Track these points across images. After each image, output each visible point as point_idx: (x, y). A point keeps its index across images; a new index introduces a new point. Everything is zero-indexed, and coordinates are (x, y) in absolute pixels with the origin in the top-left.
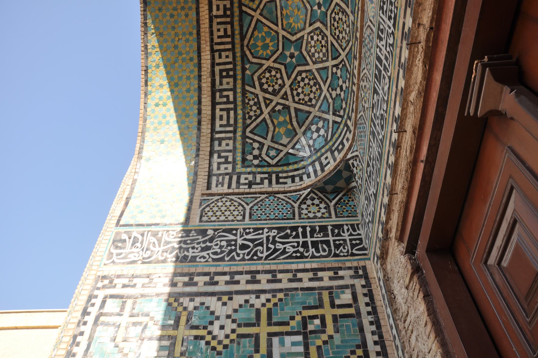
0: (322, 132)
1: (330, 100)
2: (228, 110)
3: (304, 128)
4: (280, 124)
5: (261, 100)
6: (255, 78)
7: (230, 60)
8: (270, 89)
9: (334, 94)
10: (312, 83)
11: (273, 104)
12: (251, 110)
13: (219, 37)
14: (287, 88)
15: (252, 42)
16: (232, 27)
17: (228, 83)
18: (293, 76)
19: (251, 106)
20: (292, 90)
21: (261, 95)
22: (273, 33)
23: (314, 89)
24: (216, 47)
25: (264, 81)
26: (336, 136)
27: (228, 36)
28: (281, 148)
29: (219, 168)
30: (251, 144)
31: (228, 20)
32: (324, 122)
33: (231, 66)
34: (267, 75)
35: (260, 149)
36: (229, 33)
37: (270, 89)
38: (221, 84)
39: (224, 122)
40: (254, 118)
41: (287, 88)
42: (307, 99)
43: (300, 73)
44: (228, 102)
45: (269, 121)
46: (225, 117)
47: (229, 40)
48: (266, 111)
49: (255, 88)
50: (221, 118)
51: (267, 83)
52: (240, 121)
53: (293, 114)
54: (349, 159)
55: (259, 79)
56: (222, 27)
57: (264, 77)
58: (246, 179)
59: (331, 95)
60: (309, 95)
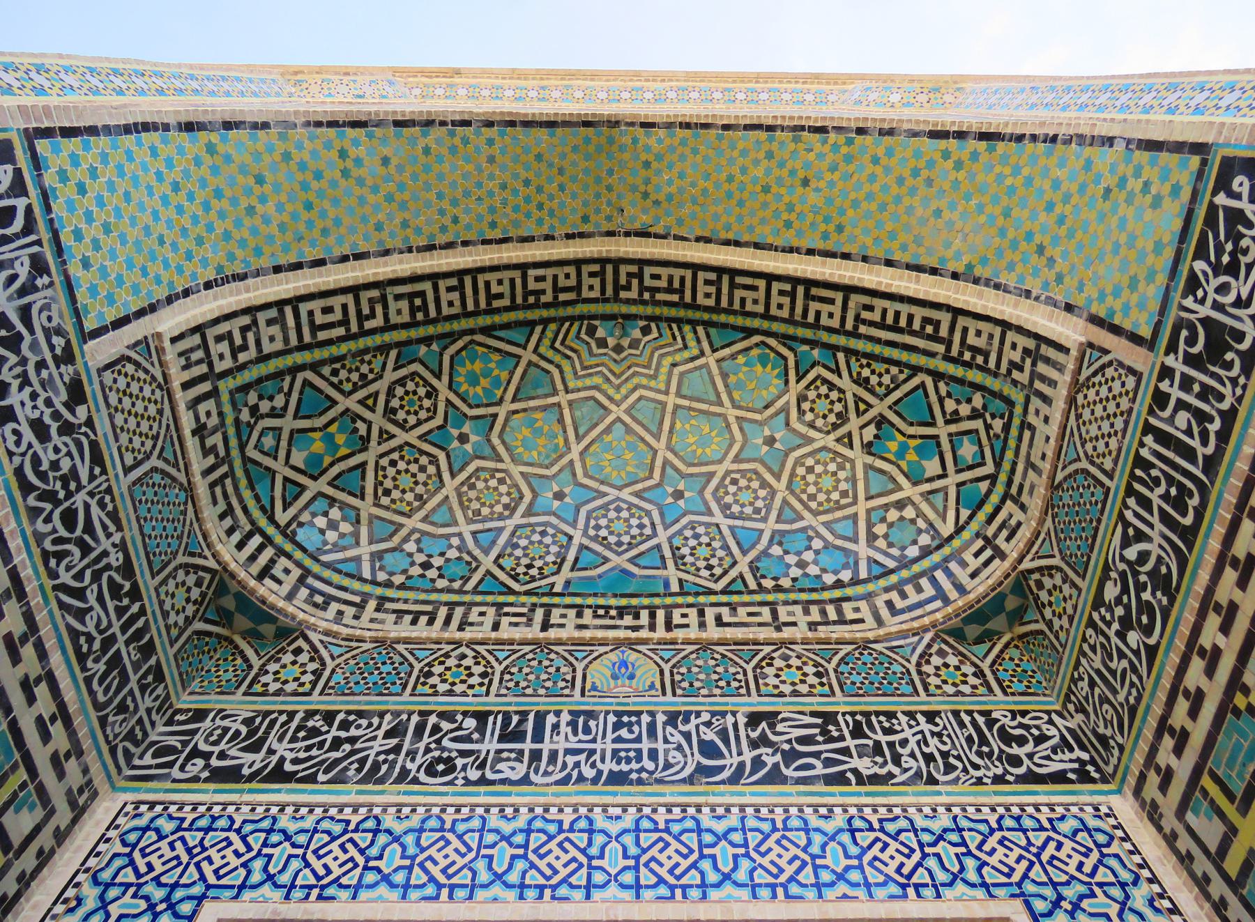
0: (331, 536)
2: (345, 322)
3: (330, 491)
4: (329, 439)
5: (372, 388)
8: (395, 403)
9: (411, 547)
11: (367, 414)
13: (487, 284)
14: (402, 437)
15: (480, 349)
16: (507, 309)
17: (399, 312)
20: (400, 448)
21: (381, 386)
22: (499, 393)
24: (468, 281)
25: (410, 386)
28: (282, 454)
30: (280, 390)
31: (519, 300)
33: (433, 313)
34: (422, 391)
35: (273, 414)
37: (395, 403)
38: (398, 297)
39: (320, 319)
41: (402, 437)
42: (388, 484)
44: (361, 318)
45: (331, 414)
47: (483, 305)
48: (351, 403)
50: (327, 310)
52: (325, 353)
53: (353, 462)
54: (306, 639)
55: (413, 375)
56: (505, 289)
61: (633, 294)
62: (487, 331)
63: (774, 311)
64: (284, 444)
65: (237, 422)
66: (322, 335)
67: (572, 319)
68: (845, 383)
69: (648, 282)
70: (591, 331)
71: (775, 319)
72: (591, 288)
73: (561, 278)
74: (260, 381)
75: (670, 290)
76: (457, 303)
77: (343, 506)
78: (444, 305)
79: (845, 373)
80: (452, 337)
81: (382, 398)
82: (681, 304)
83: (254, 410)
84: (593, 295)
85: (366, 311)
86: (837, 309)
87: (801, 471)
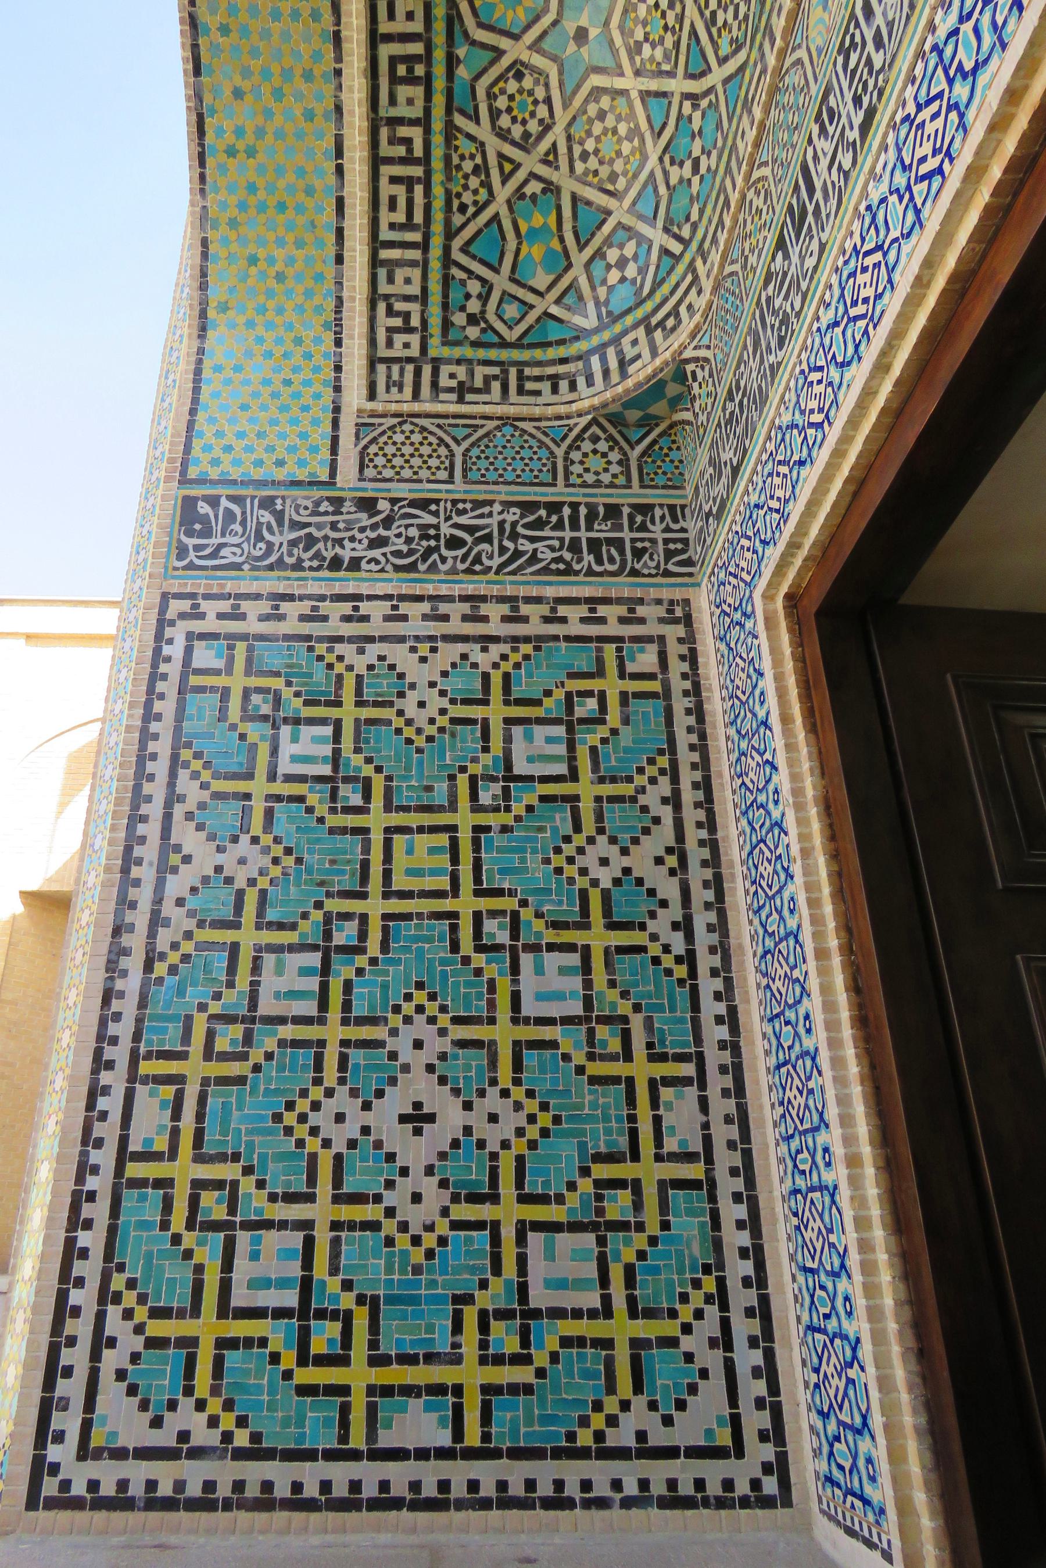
0: (631, 271)
1: (662, 190)
2: (409, 182)
3: (589, 252)
4: (533, 232)
5: (493, 161)
6: (481, 93)
10: (623, 129)
11: (521, 175)
18: (577, 102)
19: (466, 177)
21: (493, 144)
23: (626, 148)
25: (502, 103)
26: (665, 289)
28: (530, 298)
29: (390, 344)
30: (463, 283)
32: (639, 244)
34: (512, 86)
35: (484, 298)
37: (517, 131)
39: (400, 217)
41: (557, 134)
42: (604, 171)
43: (597, 93)
45: (507, 224)
48: (503, 193)
49: (478, 122)
50: (393, 206)
52: (438, 216)
55: (491, 96)
57: (503, 92)
58: (452, 376)
59: (666, 174)
60: (611, 162)
64: (521, 293)
65: (476, 344)
66: (418, 218)
74: (445, 306)
77: (608, 242)
81: (508, 150)
83: (472, 320)
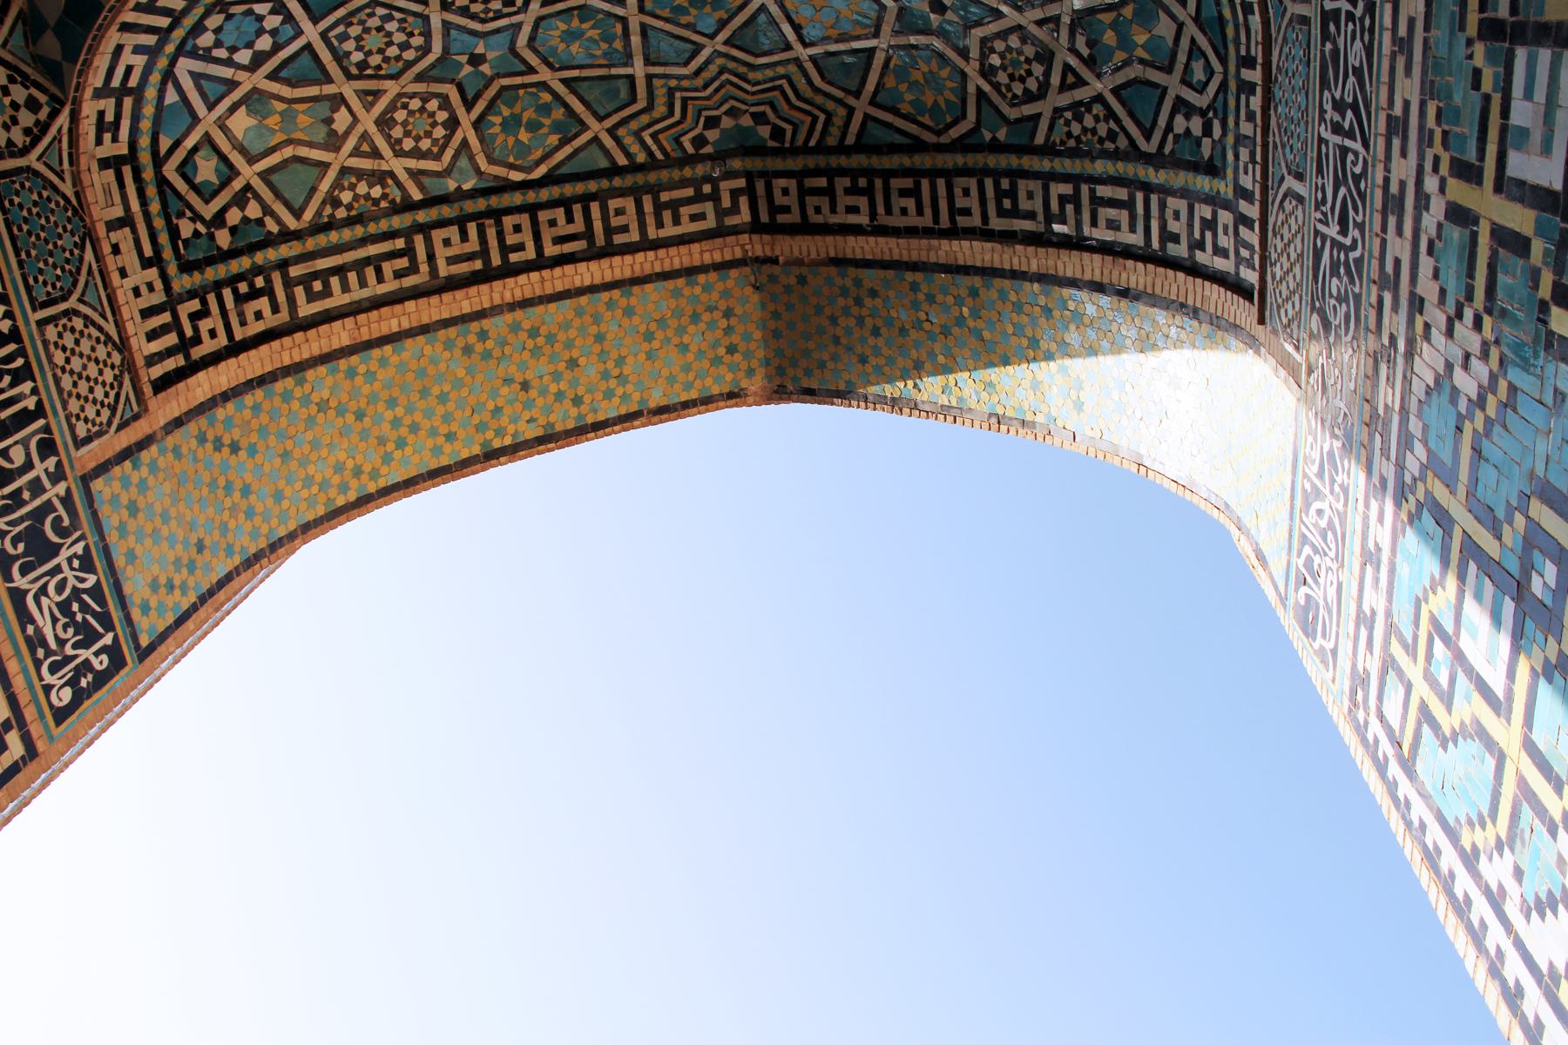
5: (1064, 100)
6: (1013, 114)
7: (973, 183)
8: (1038, 70)
11: (1073, 61)
12: (1094, 131)
17: (1030, 196)
19: (1085, 130)
24: (945, 222)
25: (1018, 89)
27: (918, 184)
31: (878, 183)
33: (989, 182)
36: (908, 183)
38: (1031, 216)
40: (1112, 125)
44: (1075, 199)
46: (1112, 213)
47: (925, 183)
49: (1040, 115)
51: (1022, 80)
56: (898, 202)
61: (726, 186)
62: (919, 146)
63: (524, 220)
67: (806, 150)
68: (398, 166)
69: (709, 207)
70: (777, 133)
71: (519, 210)
72: (785, 192)
73: (826, 209)
75: (675, 205)
76: (958, 192)
78: (974, 192)
79: (403, 176)
80: (961, 145)
81: (1055, 80)
82: (654, 190)
84: (783, 182)
85: (1070, 208)
86: (441, 253)
87: (417, 41)
